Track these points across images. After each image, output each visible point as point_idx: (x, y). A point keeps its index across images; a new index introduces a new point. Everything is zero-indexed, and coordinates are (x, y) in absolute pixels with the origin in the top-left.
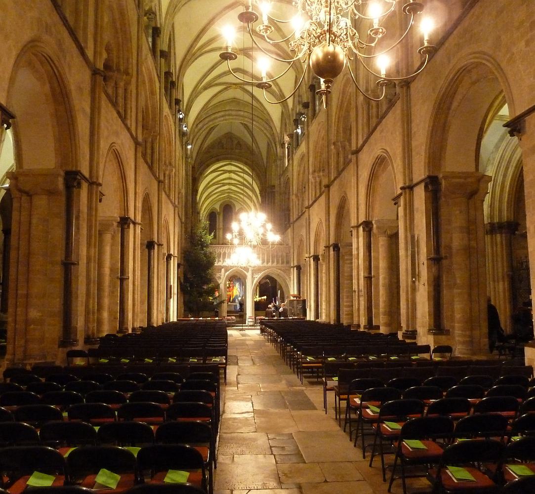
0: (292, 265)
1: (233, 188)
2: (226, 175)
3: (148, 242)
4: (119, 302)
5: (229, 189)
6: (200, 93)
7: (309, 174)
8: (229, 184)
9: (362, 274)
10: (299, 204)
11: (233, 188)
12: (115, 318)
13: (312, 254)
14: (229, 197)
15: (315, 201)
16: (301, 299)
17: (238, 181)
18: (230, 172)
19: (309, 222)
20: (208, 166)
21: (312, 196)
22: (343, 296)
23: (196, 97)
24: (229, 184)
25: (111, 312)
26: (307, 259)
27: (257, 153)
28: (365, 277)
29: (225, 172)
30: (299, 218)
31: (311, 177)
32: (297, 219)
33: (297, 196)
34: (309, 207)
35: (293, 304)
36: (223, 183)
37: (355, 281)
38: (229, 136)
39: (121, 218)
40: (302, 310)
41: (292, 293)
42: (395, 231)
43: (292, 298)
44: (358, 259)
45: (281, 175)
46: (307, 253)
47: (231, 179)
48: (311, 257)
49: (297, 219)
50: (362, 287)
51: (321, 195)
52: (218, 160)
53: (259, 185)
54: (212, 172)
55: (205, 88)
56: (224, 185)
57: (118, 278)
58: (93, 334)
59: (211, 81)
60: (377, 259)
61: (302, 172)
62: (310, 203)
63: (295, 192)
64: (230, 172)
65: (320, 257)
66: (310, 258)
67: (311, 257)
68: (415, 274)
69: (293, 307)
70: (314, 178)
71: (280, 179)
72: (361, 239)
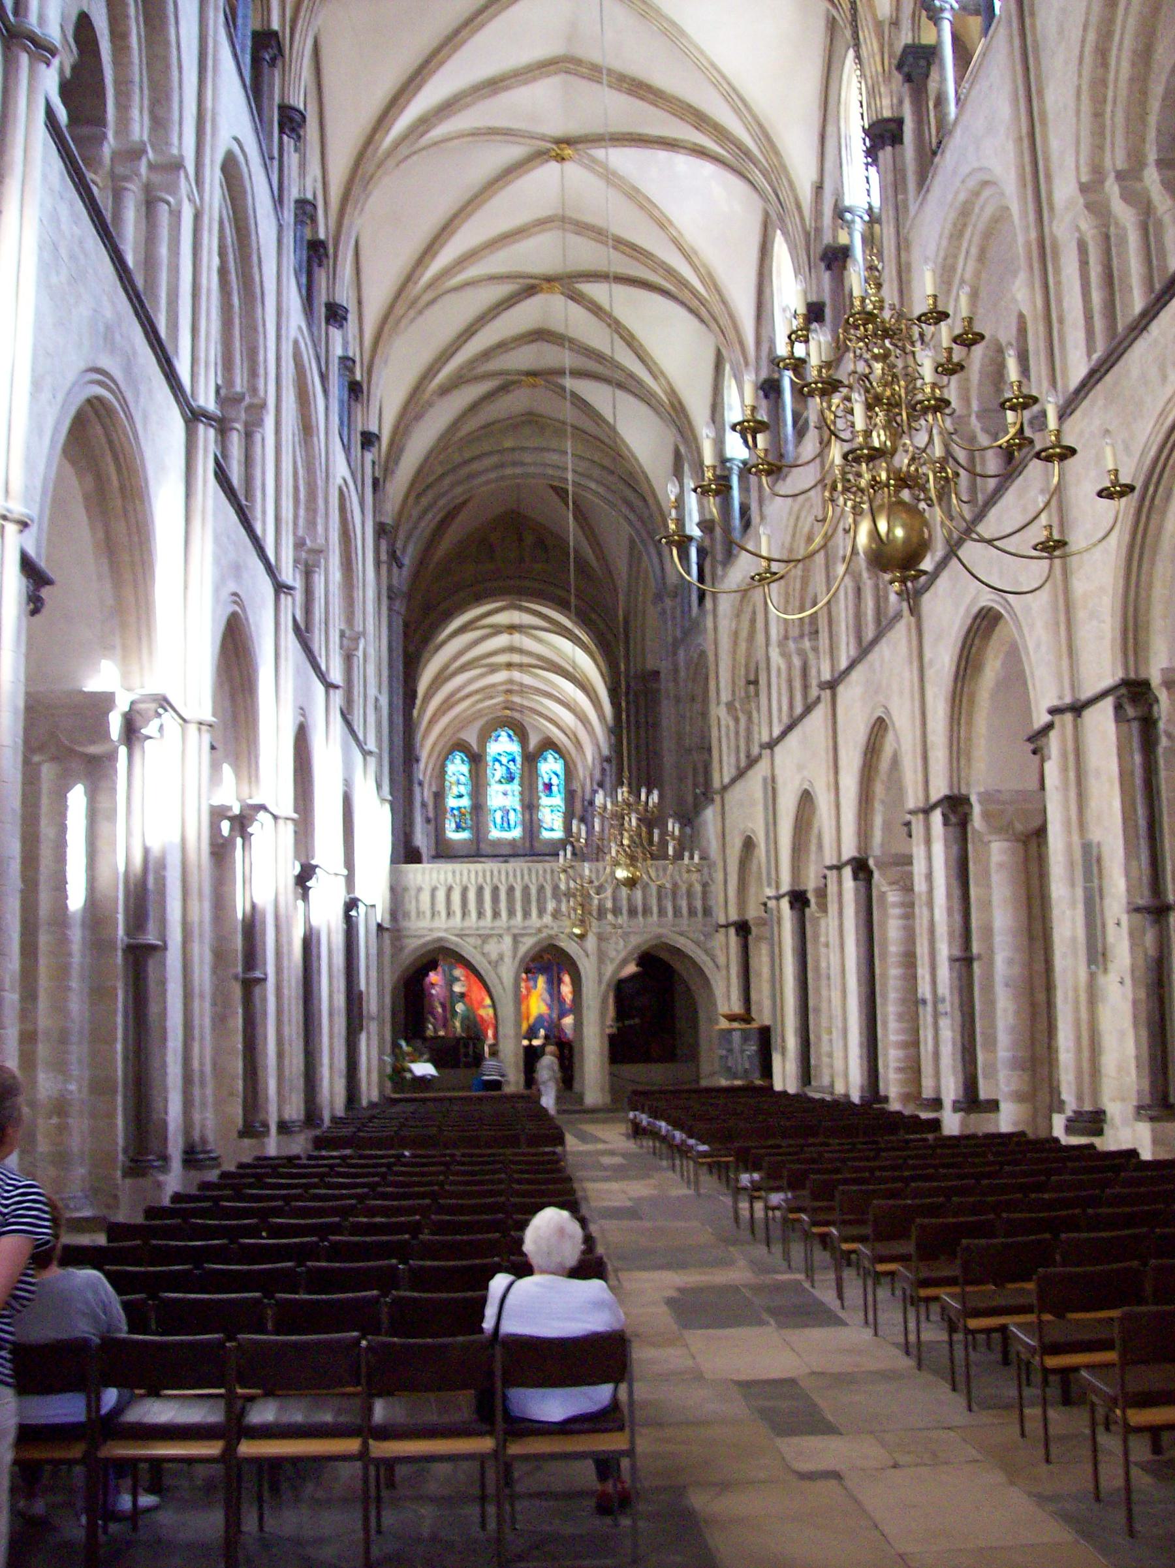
0: (722, 921)
2: (502, 640)
6: (430, 404)
7: (767, 645)
8: (509, 666)
9: (944, 951)
10: (737, 733)
11: (527, 679)
13: (785, 887)
14: (509, 706)
15: (790, 728)
16: (755, 1025)
17: (539, 657)
18: (512, 628)
19: (774, 790)
20: (448, 616)
21: (780, 710)
22: (885, 1016)
24: (509, 666)
26: (772, 904)
27: (599, 573)
28: (953, 960)
29: (497, 630)
30: (741, 774)
31: (774, 653)
32: (733, 781)
33: (730, 706)
34: (771, 745)
35: (730, 1042)
37: (923, 972)
40: (756, 1061)
41: (723, 1008)
42: (1036, 824)
43: (724, 1024)
44: (930, 904)
45: (676, 644)
46: (769, 885)
47: (512, 649)
48: (783, 896)
49: (733, 781)
50: (944, 988)
51: (808, 709)
52: (478, 599)
53: (604, 670)
54: (462, 629)
56: (494, 669)
59: (461, 368)
60: (987, 905)
61: (744, 634)
62: (776, 732)
63: (725, 696)
64: (512, 628)
65: (811, 897)
66: (778, 898)
67: (783, 896)
68: (1097, 954)
69: (730, 1050)
70: (785, 655)
71: (675, 654)
72: (938, 848)
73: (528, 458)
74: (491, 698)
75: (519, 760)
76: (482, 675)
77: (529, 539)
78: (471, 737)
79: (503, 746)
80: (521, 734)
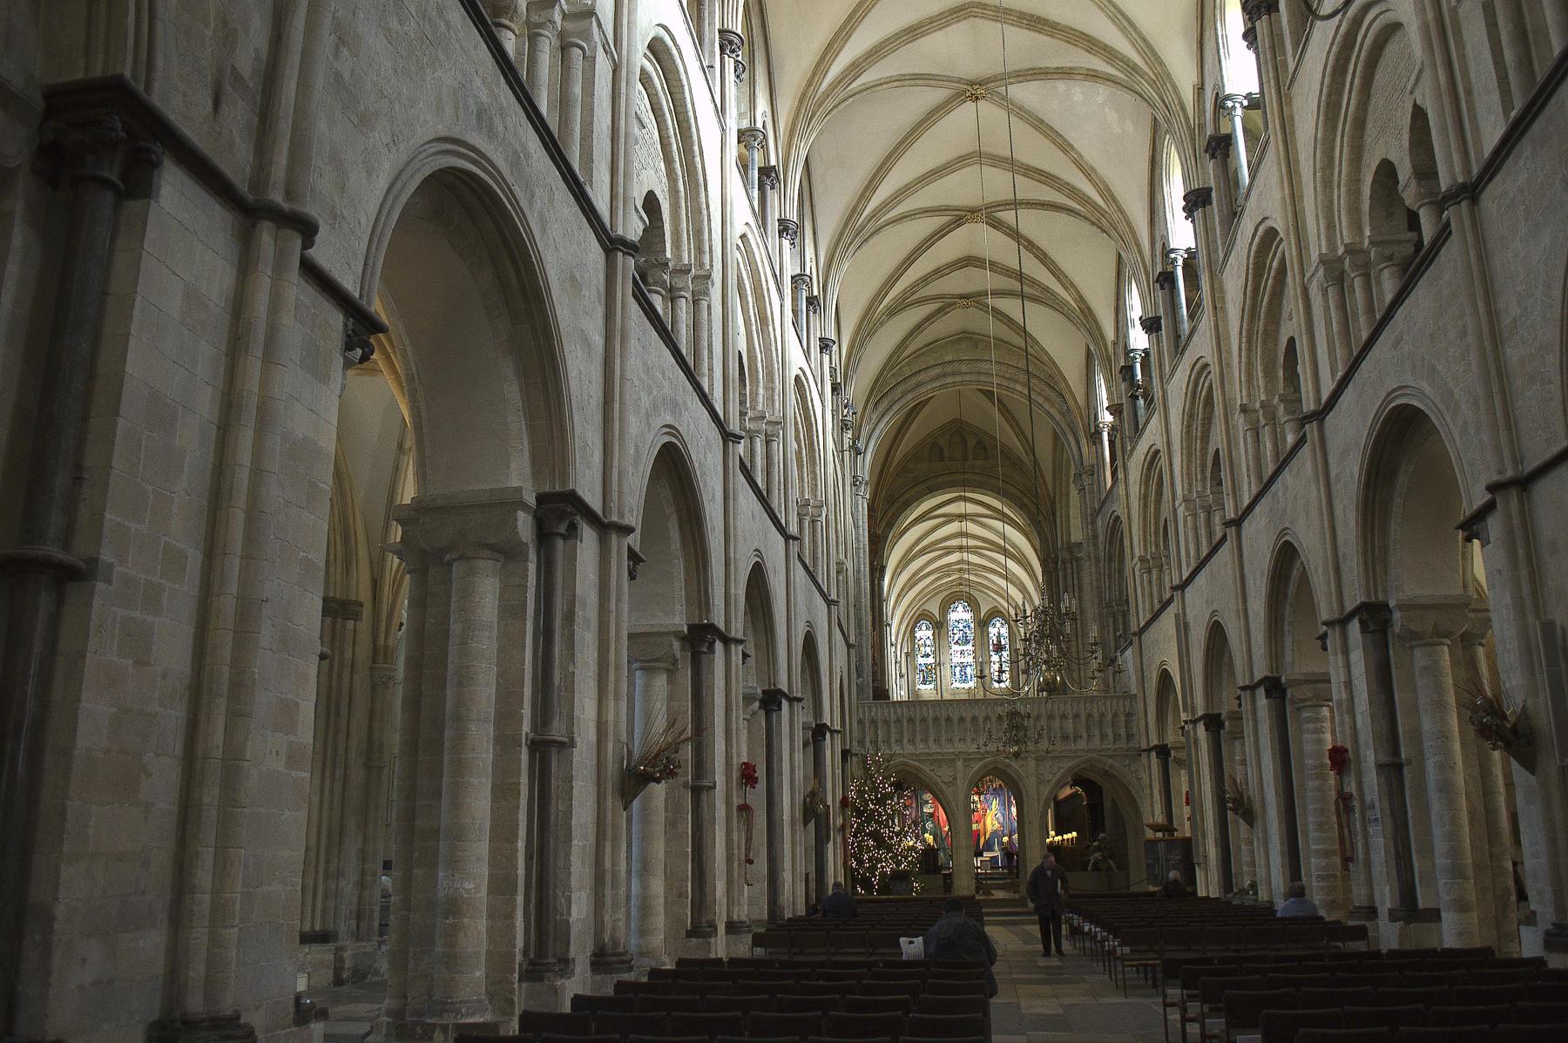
1: (974, 559)
3: (764, 692)
4: (689, 850)
5: (962, 561)
11: (974, 559)
12: (680, 896)
18: (962, 517)
23: (871, 333)
25: (671, 878)
36: (946, 548)
38: (958, 429)
39: (690, 627)
52: (932, 490)
55: (893, 312)
57: (685, 785)
58: (615, 942)
64: (962, 517)
73: (964, 368)
74: (949, 576)
75: (972, 625)
76: (940, 557)
77: (971, 442)
78: (934, 608)
79: (960, 615)
80: (973, 605)
